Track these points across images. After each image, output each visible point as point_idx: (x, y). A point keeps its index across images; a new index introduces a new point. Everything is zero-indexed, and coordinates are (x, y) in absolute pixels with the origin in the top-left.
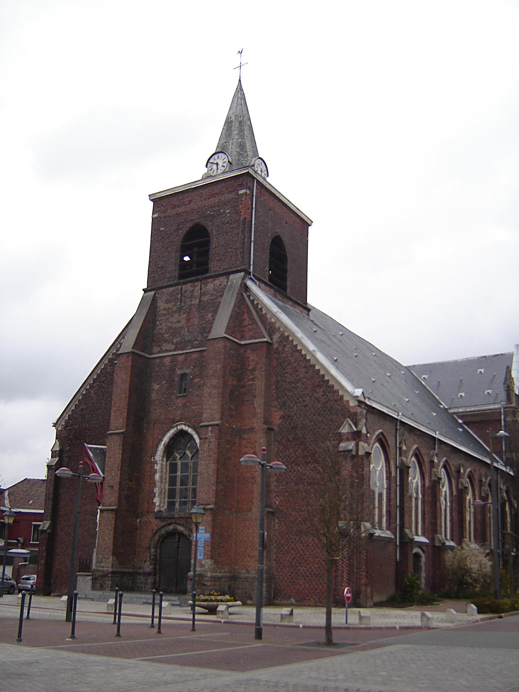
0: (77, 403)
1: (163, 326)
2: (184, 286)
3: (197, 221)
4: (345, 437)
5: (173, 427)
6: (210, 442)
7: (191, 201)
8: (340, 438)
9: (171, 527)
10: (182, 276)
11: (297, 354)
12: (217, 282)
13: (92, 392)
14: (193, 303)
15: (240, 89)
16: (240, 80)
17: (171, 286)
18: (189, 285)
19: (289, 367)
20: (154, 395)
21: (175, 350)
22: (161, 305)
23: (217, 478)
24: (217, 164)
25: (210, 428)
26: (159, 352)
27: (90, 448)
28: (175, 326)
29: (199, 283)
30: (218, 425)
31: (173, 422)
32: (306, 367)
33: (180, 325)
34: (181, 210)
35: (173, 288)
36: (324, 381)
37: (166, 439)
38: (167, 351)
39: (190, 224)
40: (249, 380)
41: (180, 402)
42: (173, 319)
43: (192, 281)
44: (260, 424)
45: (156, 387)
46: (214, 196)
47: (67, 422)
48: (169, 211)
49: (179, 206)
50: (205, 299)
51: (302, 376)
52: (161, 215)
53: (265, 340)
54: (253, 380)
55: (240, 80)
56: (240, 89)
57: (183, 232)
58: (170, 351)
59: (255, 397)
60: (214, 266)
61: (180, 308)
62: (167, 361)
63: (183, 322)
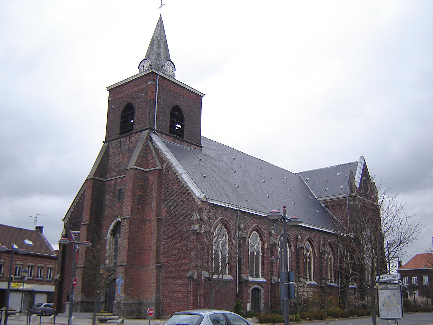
0: (74, 207)
1: (112, 163)
2: (122, 139)
3: (128, 101)
4: (194, 222)
5: (115, 220)
6: (125, 228)
8: (192, 223)
10: (121, 133)
11: (174, 175)
12: (137, 136)
13: (81, 201)
14: (126, 148)
15: (160, 20)
16: (161, 15)
17: (116, 139)
18: (124, 138)
19: (170, 183)
20: (107, 202)
21: (117, 176)
22: (111, 150)
23: (128, 248)
24: (144, 66)
25: (126, 220)
26: (110, 177)
27: (74, 233)
28: (118, 162)
29: (128, 137)
30: (129, 218)
31: (115, 217)
33: (119, 161)
34: (121, 95)
35: (116, 141)
36: (186, 190)
37: (112, 226)
38: (113, 176)
39: (125, 103)
41: (118, 205)
42: (117, 158)
43: (125, 136)
44: (154, 216)
45: (107, 197)
46: (136, 86)
47: (69, 219)
48: (116, 96)
49: (121, 93)
50: (131, 146)
51: (176, 188)
52: (113, 99)
53: (158, 168)
54: (151, 191)
55: (161, 15)
56: (160, 20)
57: (122, 108)
59: (152, 201)
61: (120, 152)
62: (113, 182)
63: (121, 160)
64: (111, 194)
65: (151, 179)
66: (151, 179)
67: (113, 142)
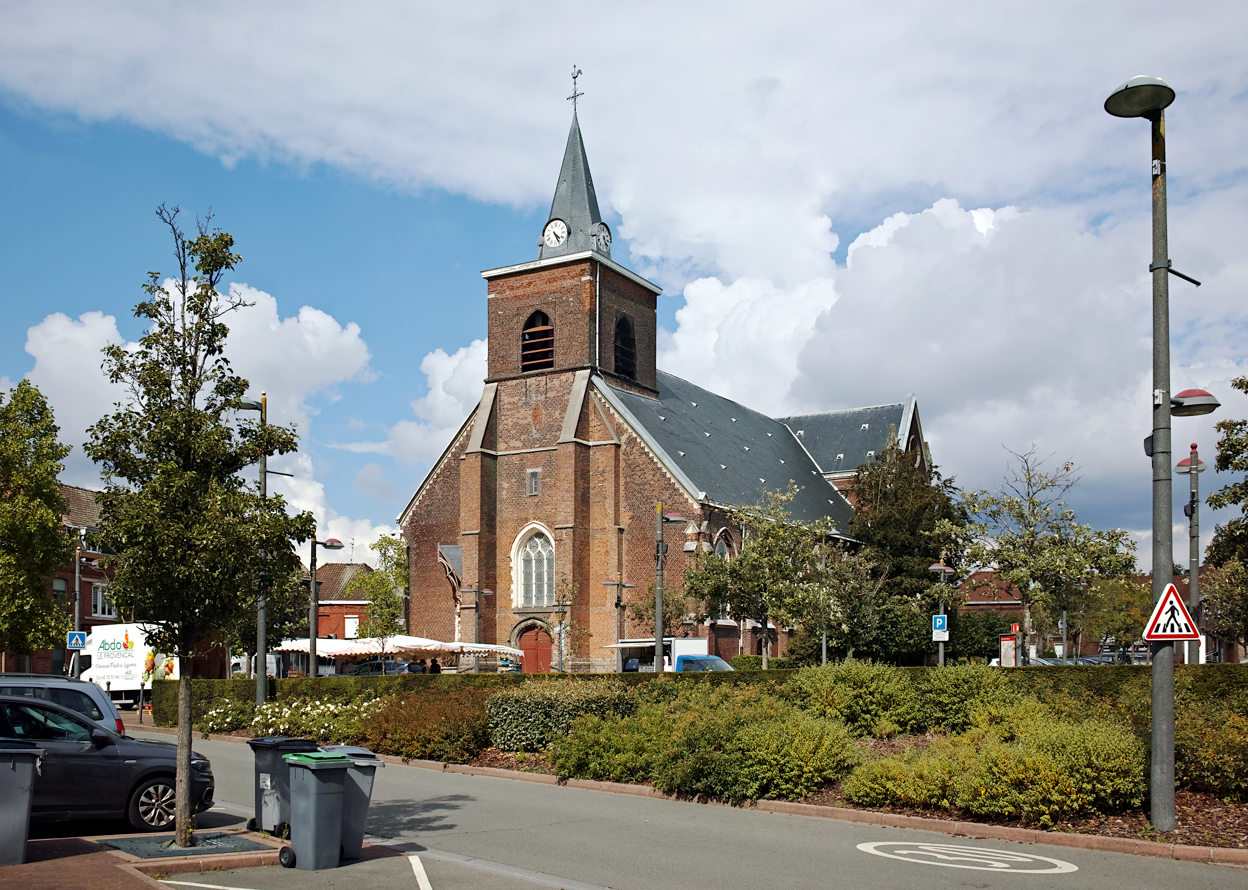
0: (421, 498)
2: (528, 380)
7: (530, 283)
8: (685, 538)
9: (530, 622)
11: (644, 456)
13: (437, 487)
15: (576, 138)
17: (514, 379)
19: (637, 469)
20: (504, 493)
22: (505, 398)
23: (574, 577)
28: (521, 422)
32: (653, 469)
33: (526, 422)
35: (517, 381)
39: (531, 311)
40: (599, 482)
44: (612, 525)
45: (505, 485)
49: (518, 288)
52: (498, 296)
53: (614, 442)
56: (576, 138)
58: (518, 448)
60: (559, 359)
61: (526, 404)
63: (530, 419)
64: (514, 480)
65: (601, 460)
66: (601, 460)
67: (509, 383)
